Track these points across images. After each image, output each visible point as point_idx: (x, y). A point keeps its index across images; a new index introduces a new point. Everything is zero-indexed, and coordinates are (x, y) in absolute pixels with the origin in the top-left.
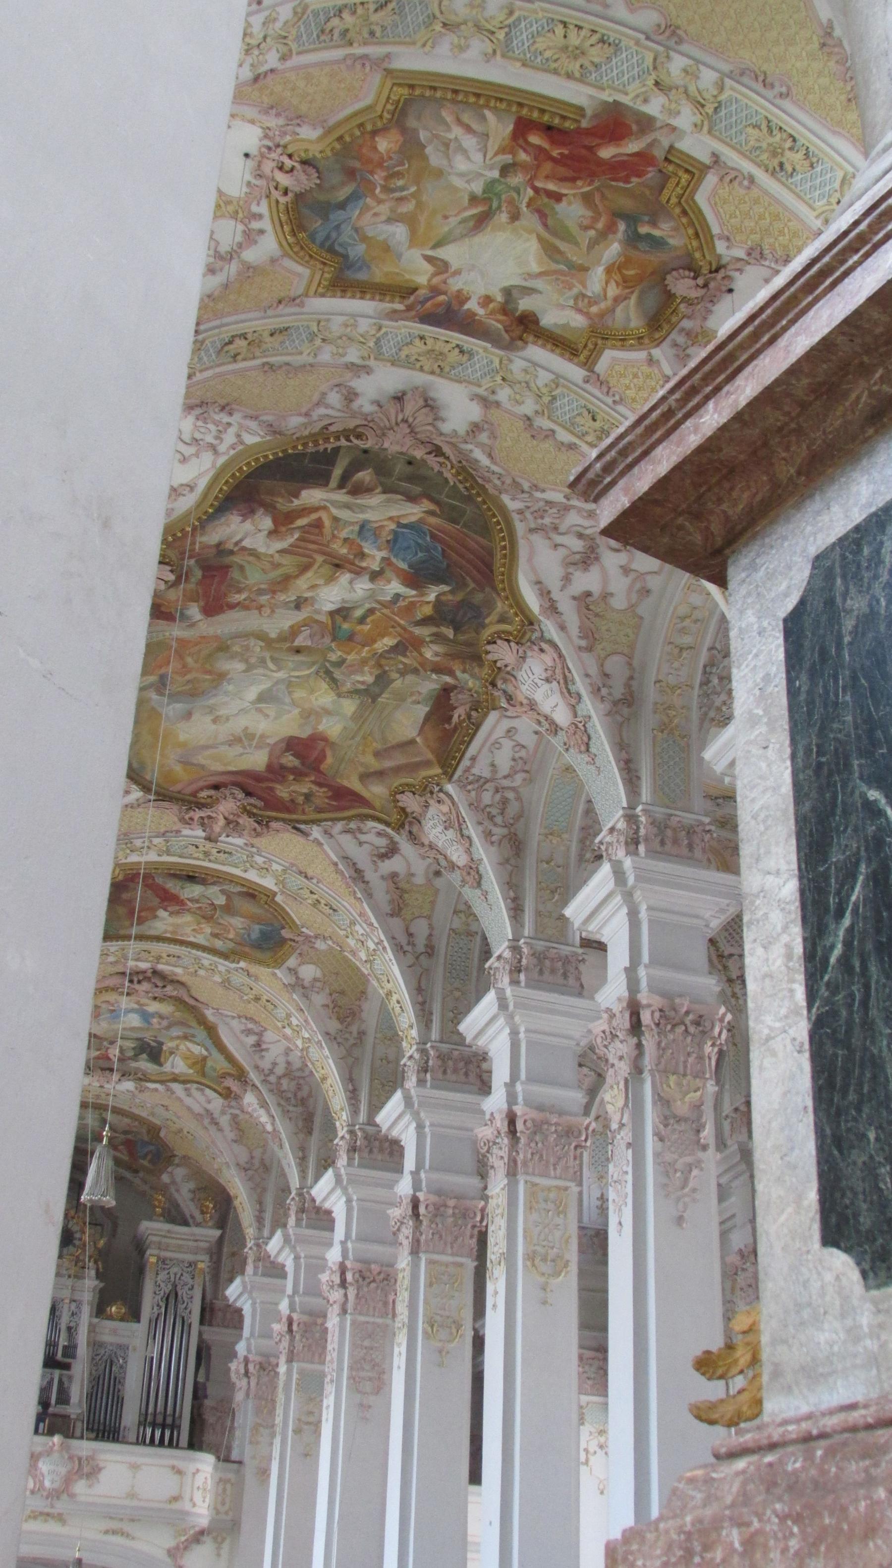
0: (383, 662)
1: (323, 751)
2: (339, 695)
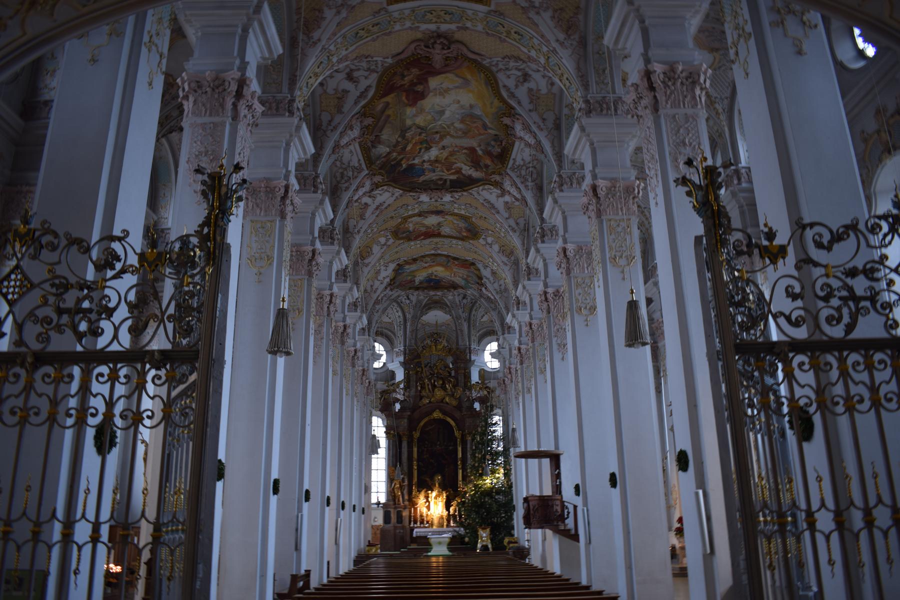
0: (406, 142)
1: (408, 100)
2: (415, 124)
